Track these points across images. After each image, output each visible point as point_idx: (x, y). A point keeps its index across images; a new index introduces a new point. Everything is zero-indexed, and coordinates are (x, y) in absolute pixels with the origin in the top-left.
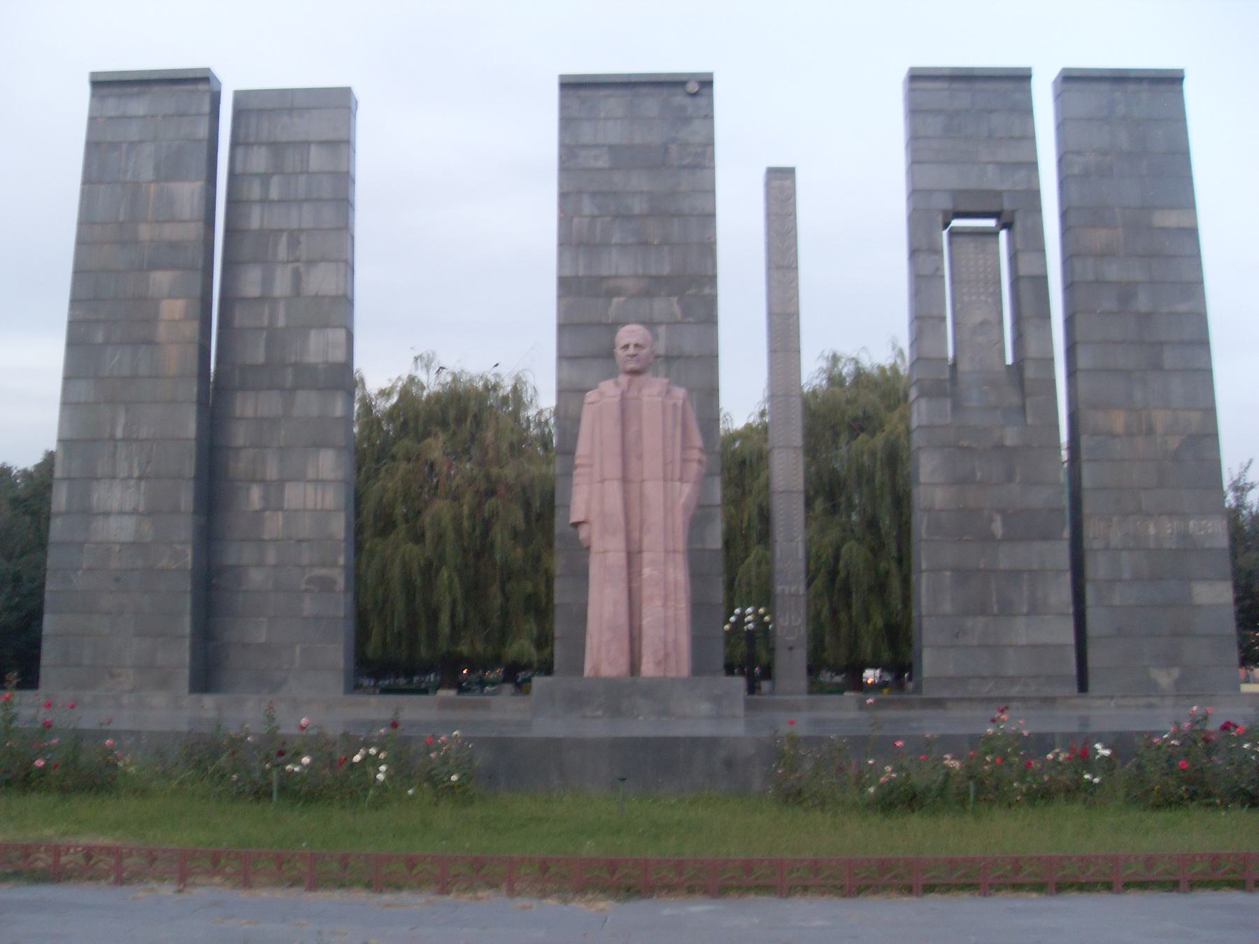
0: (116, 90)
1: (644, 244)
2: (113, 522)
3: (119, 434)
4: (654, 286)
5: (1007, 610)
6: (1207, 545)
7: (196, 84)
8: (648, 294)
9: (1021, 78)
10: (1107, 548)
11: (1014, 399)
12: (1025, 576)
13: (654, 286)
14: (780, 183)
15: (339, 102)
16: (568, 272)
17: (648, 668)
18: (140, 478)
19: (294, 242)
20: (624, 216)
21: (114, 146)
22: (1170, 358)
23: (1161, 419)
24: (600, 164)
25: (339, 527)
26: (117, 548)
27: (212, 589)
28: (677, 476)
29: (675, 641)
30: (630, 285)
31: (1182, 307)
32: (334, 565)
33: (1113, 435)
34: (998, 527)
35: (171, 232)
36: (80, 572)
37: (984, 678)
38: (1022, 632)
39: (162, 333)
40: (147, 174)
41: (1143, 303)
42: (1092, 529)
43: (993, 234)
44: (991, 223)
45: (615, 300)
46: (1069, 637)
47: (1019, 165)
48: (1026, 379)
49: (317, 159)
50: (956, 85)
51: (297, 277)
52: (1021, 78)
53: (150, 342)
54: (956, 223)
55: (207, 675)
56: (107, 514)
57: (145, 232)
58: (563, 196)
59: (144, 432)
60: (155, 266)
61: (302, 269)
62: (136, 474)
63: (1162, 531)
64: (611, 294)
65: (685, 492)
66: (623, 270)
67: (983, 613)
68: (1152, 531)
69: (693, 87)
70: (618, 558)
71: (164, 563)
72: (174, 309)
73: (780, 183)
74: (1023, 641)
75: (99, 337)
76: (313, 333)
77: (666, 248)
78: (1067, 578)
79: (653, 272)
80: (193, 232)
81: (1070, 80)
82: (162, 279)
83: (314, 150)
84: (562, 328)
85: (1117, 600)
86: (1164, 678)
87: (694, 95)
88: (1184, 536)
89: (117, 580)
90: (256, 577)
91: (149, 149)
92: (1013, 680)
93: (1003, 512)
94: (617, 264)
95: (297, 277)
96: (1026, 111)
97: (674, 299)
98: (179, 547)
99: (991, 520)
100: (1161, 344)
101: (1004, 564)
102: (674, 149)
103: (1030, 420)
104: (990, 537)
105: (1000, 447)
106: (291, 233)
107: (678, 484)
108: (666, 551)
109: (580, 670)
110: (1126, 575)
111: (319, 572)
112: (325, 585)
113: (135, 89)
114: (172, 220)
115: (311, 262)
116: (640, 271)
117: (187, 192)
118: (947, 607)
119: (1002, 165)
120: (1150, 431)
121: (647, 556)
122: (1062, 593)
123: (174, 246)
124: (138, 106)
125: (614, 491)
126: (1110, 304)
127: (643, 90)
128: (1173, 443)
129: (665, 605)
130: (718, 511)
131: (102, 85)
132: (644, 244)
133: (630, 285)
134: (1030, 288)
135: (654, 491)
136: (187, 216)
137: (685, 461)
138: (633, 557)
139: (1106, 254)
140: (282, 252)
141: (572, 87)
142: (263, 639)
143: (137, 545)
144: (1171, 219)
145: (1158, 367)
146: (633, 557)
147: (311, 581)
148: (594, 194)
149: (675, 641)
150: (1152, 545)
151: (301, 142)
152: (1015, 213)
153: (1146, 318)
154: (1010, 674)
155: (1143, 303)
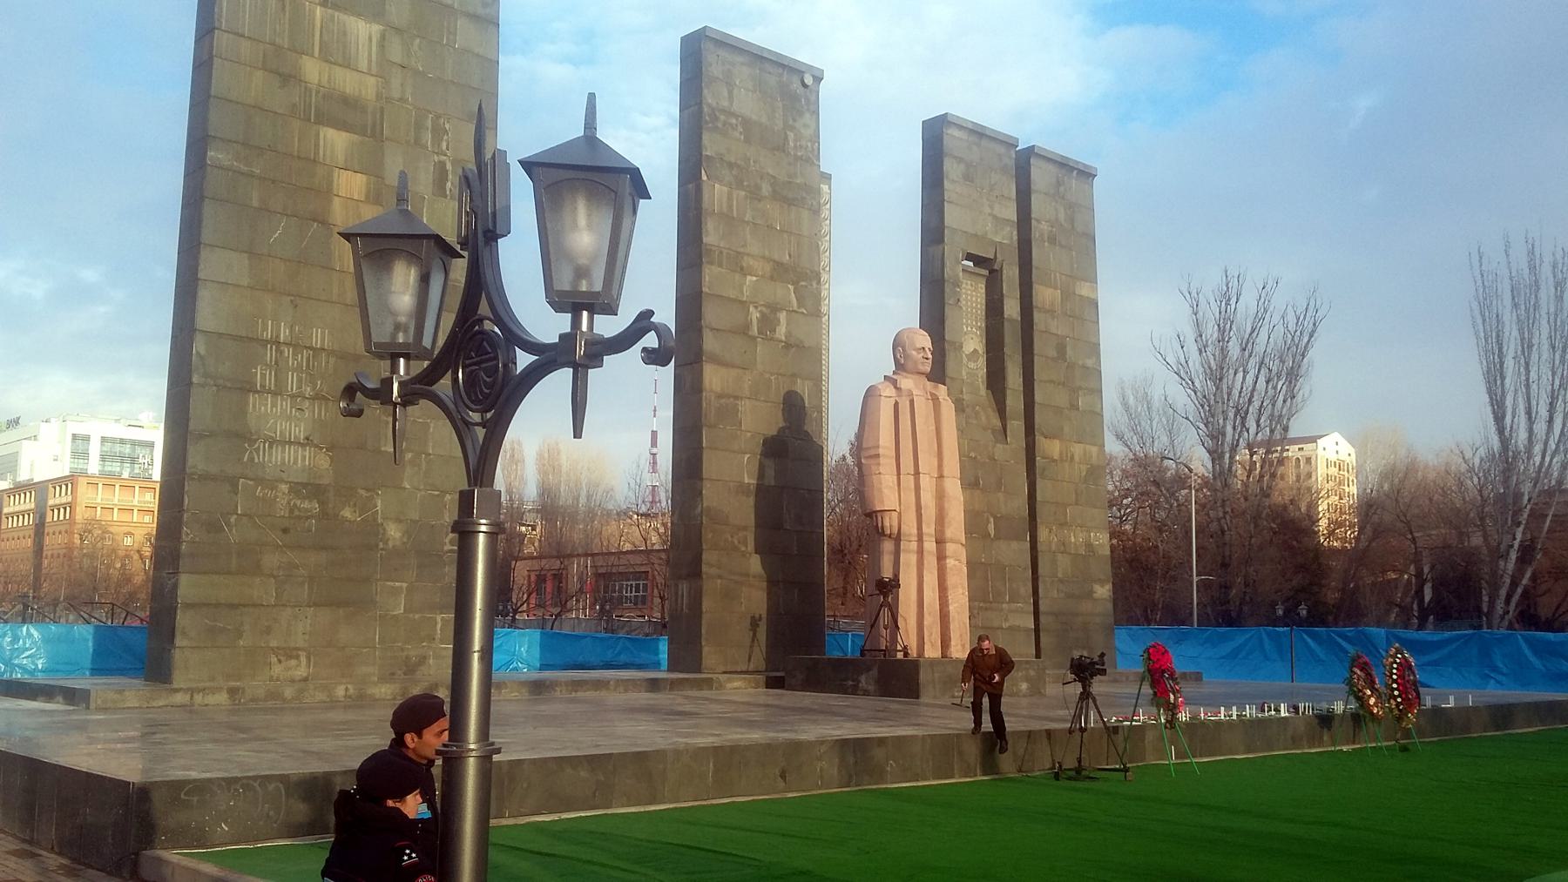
4: (781, 272)
8: (772, 278)
11: (997, 422)
13: (781, 272)
18: (313, 398)
19: (439, 132)
20: (755, 195)
23: (1077, 450)
26: (284, 487)
31: (1090, 363)
34: (991, 528)
35: (347, 82)
36: (233, 519)
42: (1043, 534)
49: (465, 34)
50: (973, 138)
57: (312, 70)
59: (318, 338)
60: (324, 119)
61: (449, 167)
62: (308, 391)
63: (1076, 538)
64: (744, 272)
69: (809, 80)
70: (929, 545)
71: (347, 513)
79: (776, 257)
82: (336, 141)
87: (805, 85)
88: (1089, 546)
89: (285, 531)
90: (394, 532)
93: (995, 518)
98: (362, 492)
100: (1080, 388)
102: (791, 135)
106: (438, 117)
114: (348, 67)
119: (995, 217)
120: (1072, 458)
121: (950, 548)
126: (1052, 353)
127: (767, 66)
128: (1084, 468)
132: (770, 227)
136: (363, 65)
139: (1051, 312)
140: (428, 138)
143: (310, 489)
145: (1074, 407)
148: (731, 165)
153: (1071, 366)
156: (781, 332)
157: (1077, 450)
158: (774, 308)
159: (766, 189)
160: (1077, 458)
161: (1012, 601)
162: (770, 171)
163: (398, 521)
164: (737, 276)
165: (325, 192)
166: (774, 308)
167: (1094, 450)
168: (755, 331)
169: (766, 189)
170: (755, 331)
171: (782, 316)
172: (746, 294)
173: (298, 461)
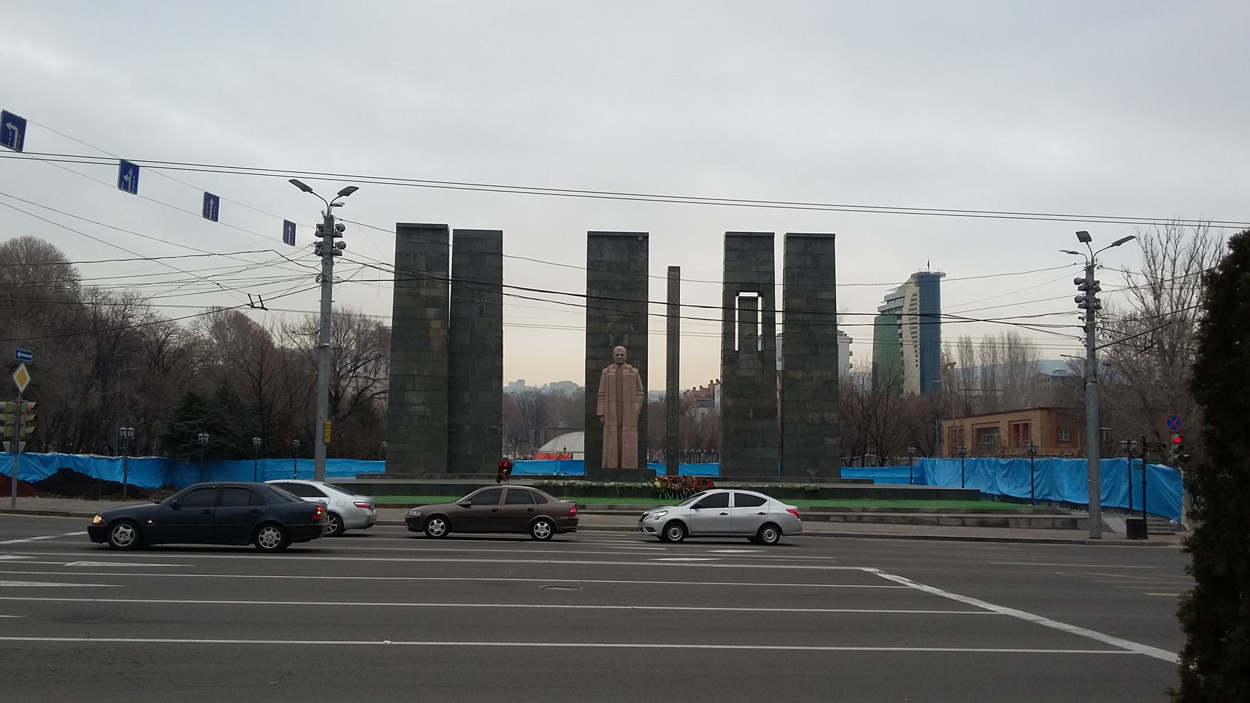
2: (414, 408)
7: (443, 229)
9: (771, 237)
11: (760, 366)
14: (674, 274)
15: (497, 237)
17: (624, 466)
23: (816, 374)
27: (453, 430)
39: (432, 333)
43: (756, 299)
44: (756, 294)
47: (767, 272)
48: (766, 358)
52: (771, 237)
54: (742, 294)
64: (606, 322)
72: (436, 324)
73: (674, 274)
81: (790, 238)
82: (431, 312)
86: (812, 472)
90: (467, 428)
96: (771, 250)
120: (812, 379)
125: (613, 406)
134: (769, 322)
138: (620, 427)
141: (593, 237)
144: (825, 295)
146: (620, 427)
151: (483, 250)
152: (767, 291)
157: (816, 374)
159: (618, 287)
167: (829, 374)
169: (618, 287)
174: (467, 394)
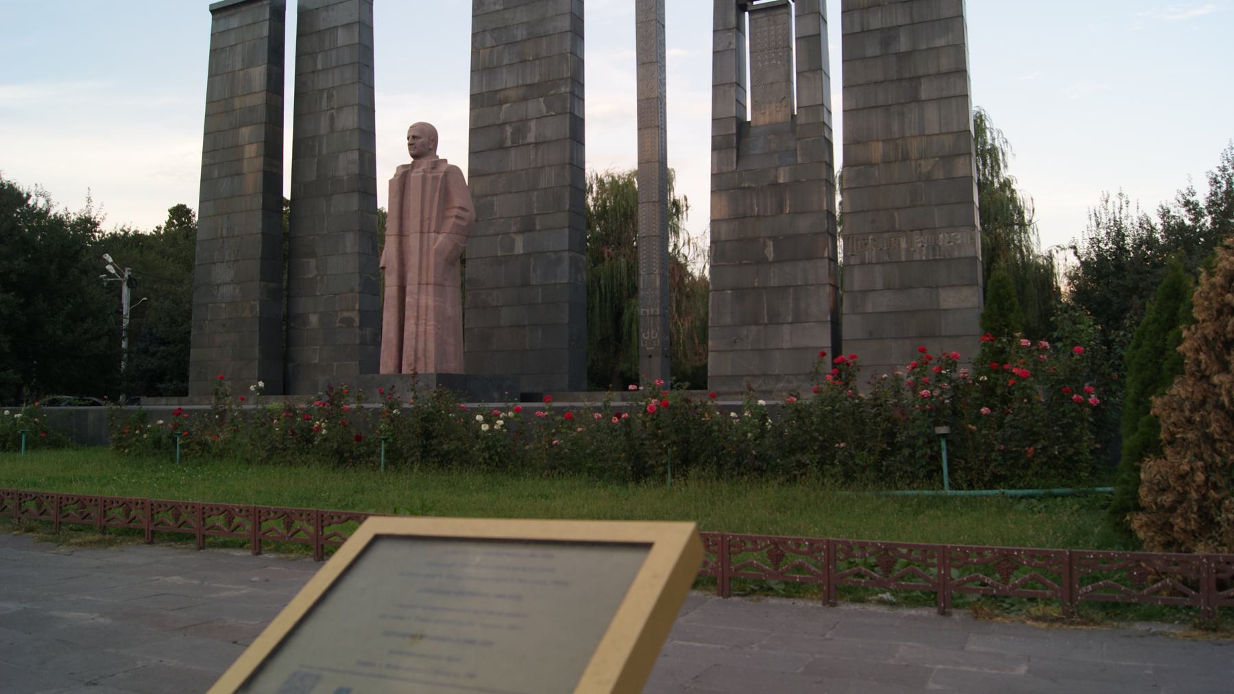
0: (225, 14)
1: (524, 61)
3: (225, 234)
5: (775, 320)
6: (956, 254)
10: (863, 263)
12: (791, 290)
16: (476, 91)
19: (330, 97)
21: (223, 49)
22: (925, 91)
23: (914, 147)
24: (498, 7)
25: (356, 283)
28: (432, 229)
29: (425, 349)
30: (512, 94)
32: (354, 309)
33: (872, 165)
34: (770, 253)
37: (755, 376)
38: (787, 337)
39: (246, 167)
40: (239, 66)
41: (903, 44)
45: (505, 106)
46: (826, 341)
51: (332, 118)
53: (240, 174)
55: (282, 383)
56: (218, 285)
57: (237, 103)
58: (474, 35)
60: (241, 126)
64: (501, 103)
65: (440, 241)
66: (509, 85)
67: (757, 323)
68: (903, 245)
74: (786, 345)
75: (216, 174)
76: (341, 156)
77: (537, 62)
78: (828, 289)
79: (529, 82)
80: (259, 99)
82: (245, 132)
83: (340, 30)
84: (472, 131)
85: (869, 308)
90: (314, 319)
91: (239, 48)
92: (778, 378)
93: (775, 239)
94: (507, 80)
95: (332, 118)
97: (541, 100)
99: (765, 246)
100: (920, 77)
101: (774, 282)
103: (799, 160)
104: (762, 261)
105: (775, 185)
107: (433, 235)
108: (420, 284)
109: (378, 372)
110: (879, 286)
111: (346, 314)
112: (348, 322)
113: (233, 11)
115: (340, 109)
116: (520, 83)
117: (259, 74)
118: (728, 320)
120: (906, 158)
121: (408, 289)
122: (820, 304)
123: (252, 109)
124: (234, 22)
129: (417, 325)
130: (566, 255)
131: (215, 11)
132: (525, 61)
133: (512, 94)
134: (814, 44)
135: (413, 242)
136: (257, 89)
137: (442, 218)
142: (317, 361)
145: (917, 100)
147: (342, 321)
148: (493, 30)
149: (425, 349)
150: (903, 259)
154: (777, 372)
155: (903, 44)
156: (531, 138)
158: (525, 121)
159: (520, 34)
160: (914, 154)
161: (796, 321)
162: (525, 20)
163: (315, 312)
164: (495, 108)
165: (240, 160)
166: (525, 121)
168: (509, 143)
169: (520, 34)
170: (509, 143)
171: (533, 124)
172: (502, 116)
173: (227, 291)
174: (313, 262)
